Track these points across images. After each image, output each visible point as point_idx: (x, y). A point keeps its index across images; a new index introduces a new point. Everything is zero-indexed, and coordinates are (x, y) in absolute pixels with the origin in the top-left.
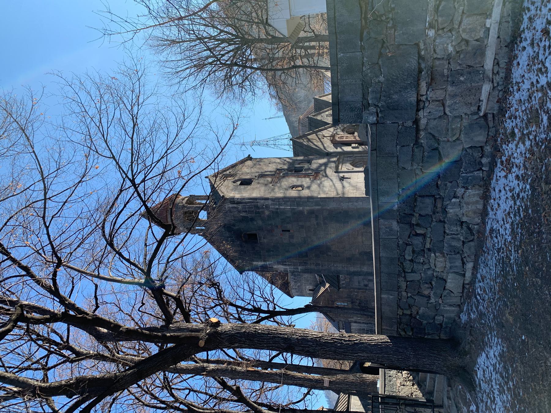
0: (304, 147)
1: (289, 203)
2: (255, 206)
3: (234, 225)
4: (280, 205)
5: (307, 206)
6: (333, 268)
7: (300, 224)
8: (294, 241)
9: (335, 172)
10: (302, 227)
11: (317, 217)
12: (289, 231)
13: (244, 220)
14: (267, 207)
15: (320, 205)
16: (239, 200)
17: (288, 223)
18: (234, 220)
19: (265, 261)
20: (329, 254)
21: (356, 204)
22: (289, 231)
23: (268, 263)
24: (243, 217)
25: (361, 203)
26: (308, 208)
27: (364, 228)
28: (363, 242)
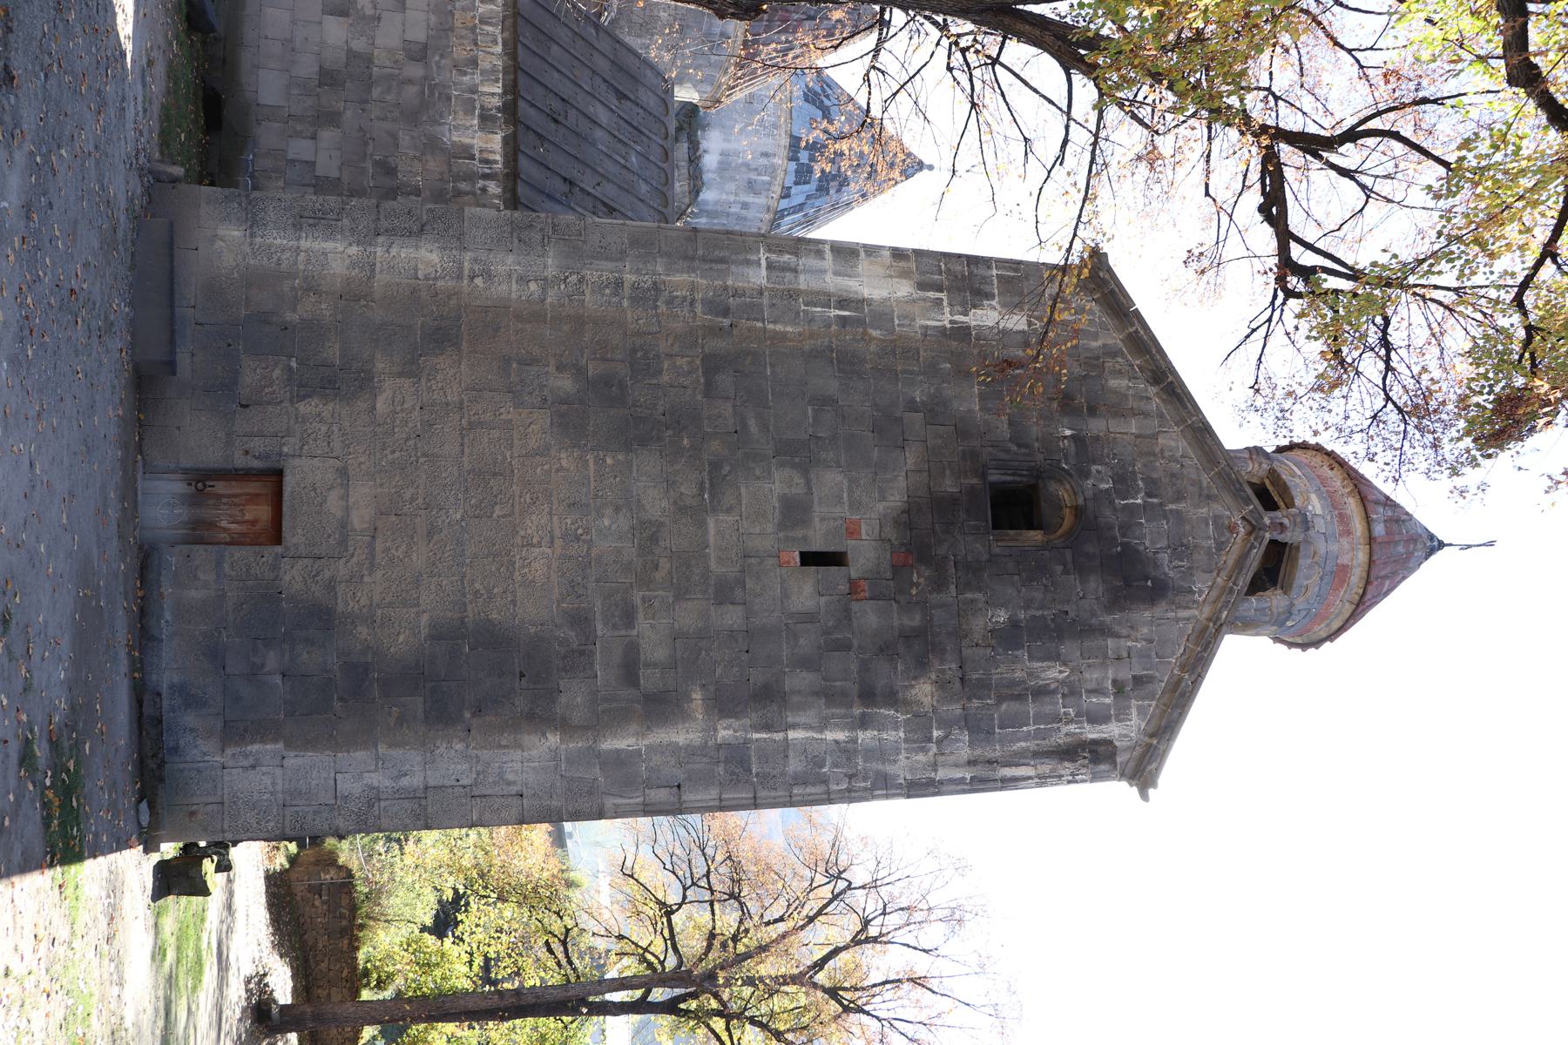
1: (795, 765)
4: (846, 751)
5: (691, 751)
6: (551, 264)
7: (732, 617)
8: (781, 483)
10: (724, 593)
11: (630, 671)
12: (808, 559)
13: (1051, 633)
14: (919, 735)
16: (1067, 768)
17: (809, 618)
19: (962, 332)
20: (565, 384)
21: (376, 779)
22: (808, 559)
24: (1055, 657)
25: (348, 785)
27: (331, 587)
28: (343, 473)
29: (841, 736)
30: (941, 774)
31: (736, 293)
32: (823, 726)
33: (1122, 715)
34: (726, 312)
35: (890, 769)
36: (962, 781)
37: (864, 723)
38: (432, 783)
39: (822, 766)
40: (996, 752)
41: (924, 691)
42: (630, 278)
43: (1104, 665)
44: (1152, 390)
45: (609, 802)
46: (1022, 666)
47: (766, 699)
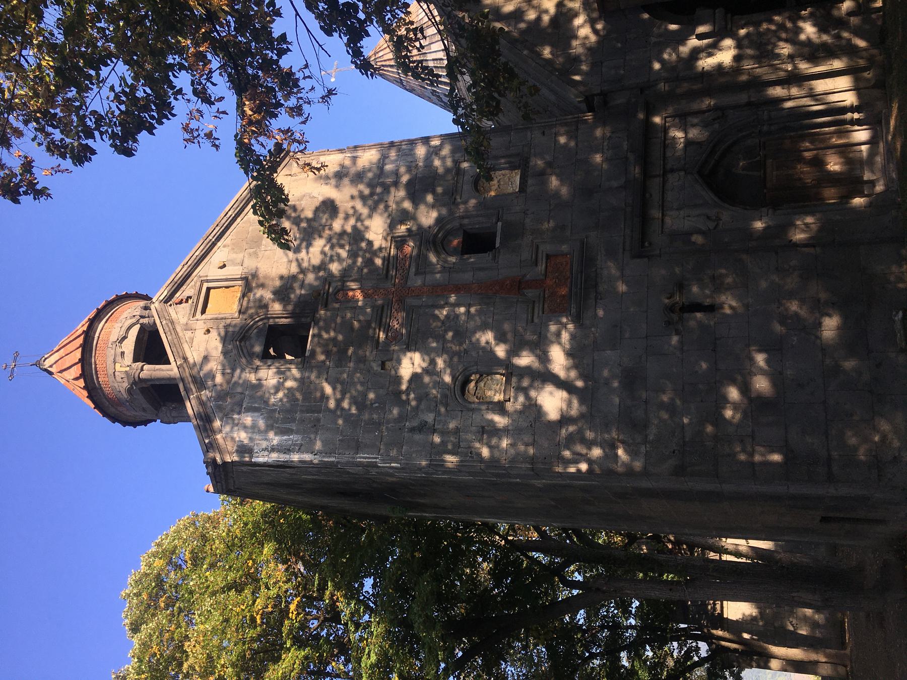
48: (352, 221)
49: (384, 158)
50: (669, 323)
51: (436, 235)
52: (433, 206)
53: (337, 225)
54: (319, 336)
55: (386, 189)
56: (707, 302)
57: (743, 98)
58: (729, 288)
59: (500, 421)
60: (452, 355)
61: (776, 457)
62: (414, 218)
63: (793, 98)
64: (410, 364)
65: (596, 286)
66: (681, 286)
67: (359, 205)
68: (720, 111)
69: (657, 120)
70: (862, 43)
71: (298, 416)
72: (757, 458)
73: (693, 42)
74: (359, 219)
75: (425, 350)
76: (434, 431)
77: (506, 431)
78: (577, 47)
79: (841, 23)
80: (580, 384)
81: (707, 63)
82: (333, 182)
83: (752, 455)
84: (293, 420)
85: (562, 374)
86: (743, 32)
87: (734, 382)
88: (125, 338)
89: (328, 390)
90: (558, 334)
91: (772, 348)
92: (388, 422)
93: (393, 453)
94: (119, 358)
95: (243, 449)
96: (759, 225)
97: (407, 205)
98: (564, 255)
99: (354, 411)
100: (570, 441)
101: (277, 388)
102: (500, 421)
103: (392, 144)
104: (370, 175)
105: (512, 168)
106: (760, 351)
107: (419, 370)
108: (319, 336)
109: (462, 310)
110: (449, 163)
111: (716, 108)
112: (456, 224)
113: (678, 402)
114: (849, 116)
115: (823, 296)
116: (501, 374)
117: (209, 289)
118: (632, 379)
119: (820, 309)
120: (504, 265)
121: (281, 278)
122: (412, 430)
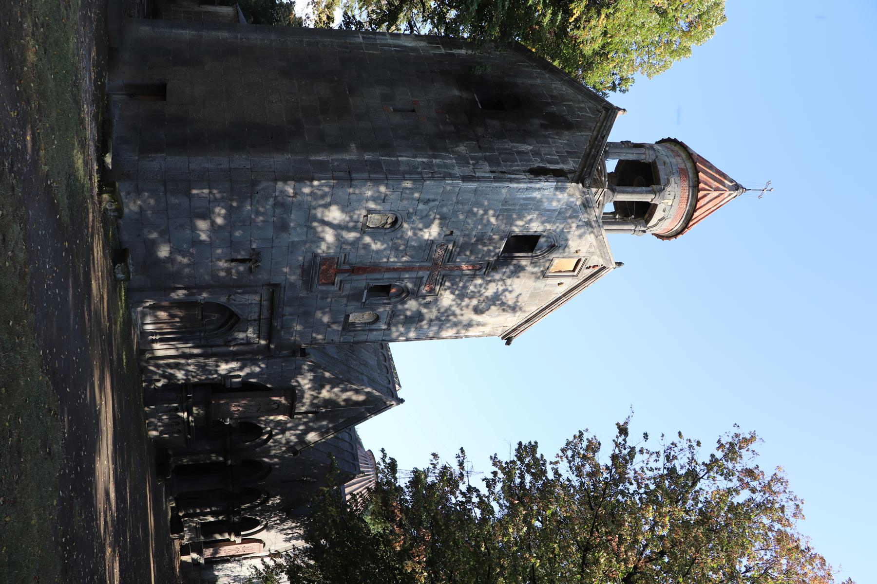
0: (365, 378)
1: (402, 168)
2: (499, 164)
3: (544, 127)
4: (430, 165)
8: (378, 90)
9: (277, 285)
15: (313, 163)
18: (545, 137)
21: (207, 165)
23: (443, 51)
24: (524, 142)
26: (347, 157)
29: (425, 160)
30: (478, 174)
31: (350, 43)
32: (416, 157)
33: (564, 162)
34: (347, 48)
35: (450, 171)
36: (489, 177)
37: (435, 157)
38: (232, 167)
39: (418, 168)
40: (504, 169)
41: (462, 149)
42: (306, 40)
43: (551, 147)
44: (543, 72)
45: (316, 175)
46: (508, 145)
47: (387, 147)
48: (464, 304)
49: (438, 332)
50: (259, 254)
51: (407, 296)
52: (407, 309)
53: (475, 302)
54: (495, 248)
55: (437, 318)
56: (233, 264)
57: (215, 350)
58: (222, 270)
59: (372, 205)
60: (402, 238)
61: (195, 192)
62: (420, 304)
63: (187, 348)
64: (433, 232)
65: (303, 271)
66: (250, 270)
67: (458, 311)
68: (227, 344)
69: (263, 342)
70: (151, 368)
71: (517, 207)
72: (206, 191)
73: (242, 374)
74: (459, 305)
75: (420, 239)
76: (419, 200)
77: (367, 200)
78: (310, 376)
79: (164, 376)
80: (315, 224)
81: (234, 365)
82: (474, 323)
83: (210, 193)
84: (521, 205)
85: (327, 229)
86: (215, 376)
87: (220, 227)
88: (660, 220)
89: (493, 220)
90: (328, 248)
91: (196, 242)
92: (451, 205)
93: (448, 188)
94: (668, 209)
95: (562, 189)
96: (205, 295)
97: (424, 311)
98: (323, 284)
99: (475, 210)
100: (323, 197)
101: (531, 221)
102: (372, 205)
103: (431, 338)
104: (448, 325)
105: (353, 324)
106: (204, 241)
107: (425, 230)
108: (495, 248)
109: (392, 260)
110: (394, 329)
111: (230, 346)
112: (393, 300)
113: (253, 216)
114: (158, 337)
115: (170, 265)
116: (368, 227)
117: (574, 271)
118: (283, 227)
119: (170, 260)
120: (362, 281)
121: (518, 277)
122: (434, 200)
